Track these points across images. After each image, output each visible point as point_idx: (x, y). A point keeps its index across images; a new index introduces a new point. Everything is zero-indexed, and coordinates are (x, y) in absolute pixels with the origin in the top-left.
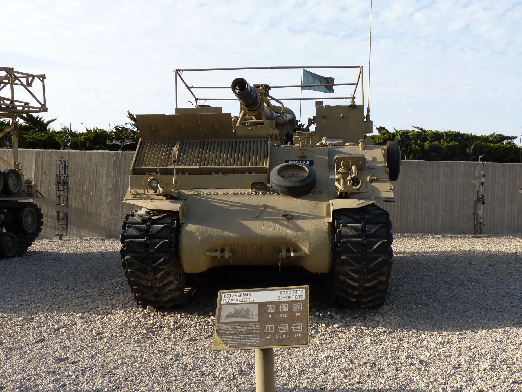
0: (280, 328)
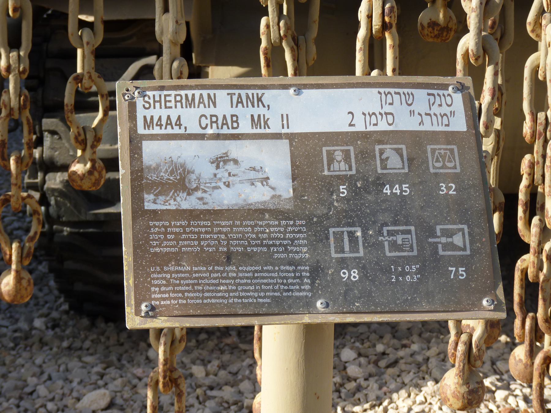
0: (385, 240)
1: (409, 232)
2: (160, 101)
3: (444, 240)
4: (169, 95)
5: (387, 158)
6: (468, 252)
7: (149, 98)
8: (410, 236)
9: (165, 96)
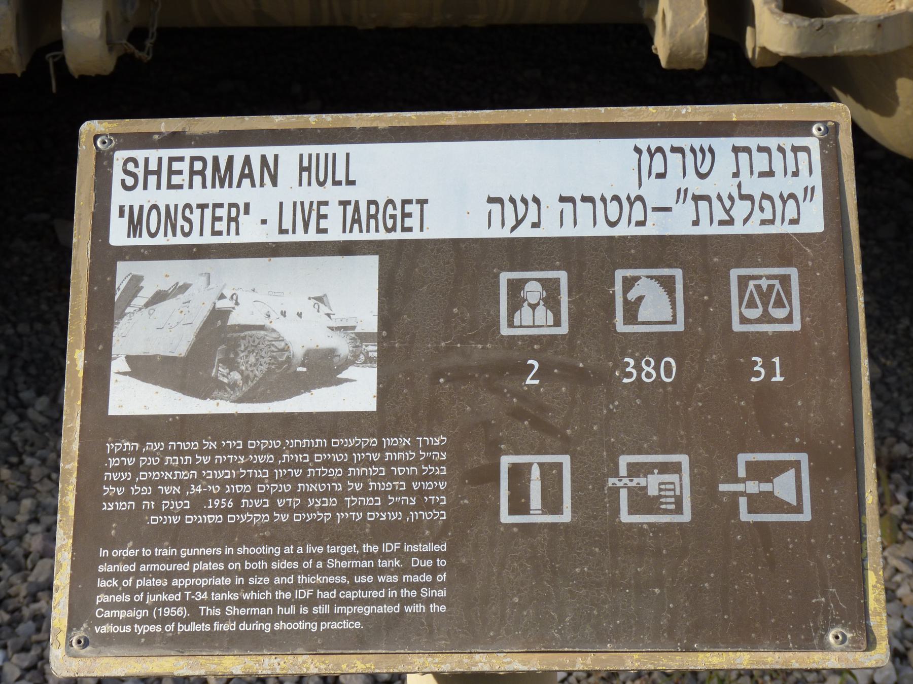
0: (622, 483)
1: (675, 468)
2: (158, 173)
3: (753, 487)
4: (181, 159)
5: (640, 299)
6: (806, 516)
7: (137, 166)
8: (677, 476)
9: (172, 160)
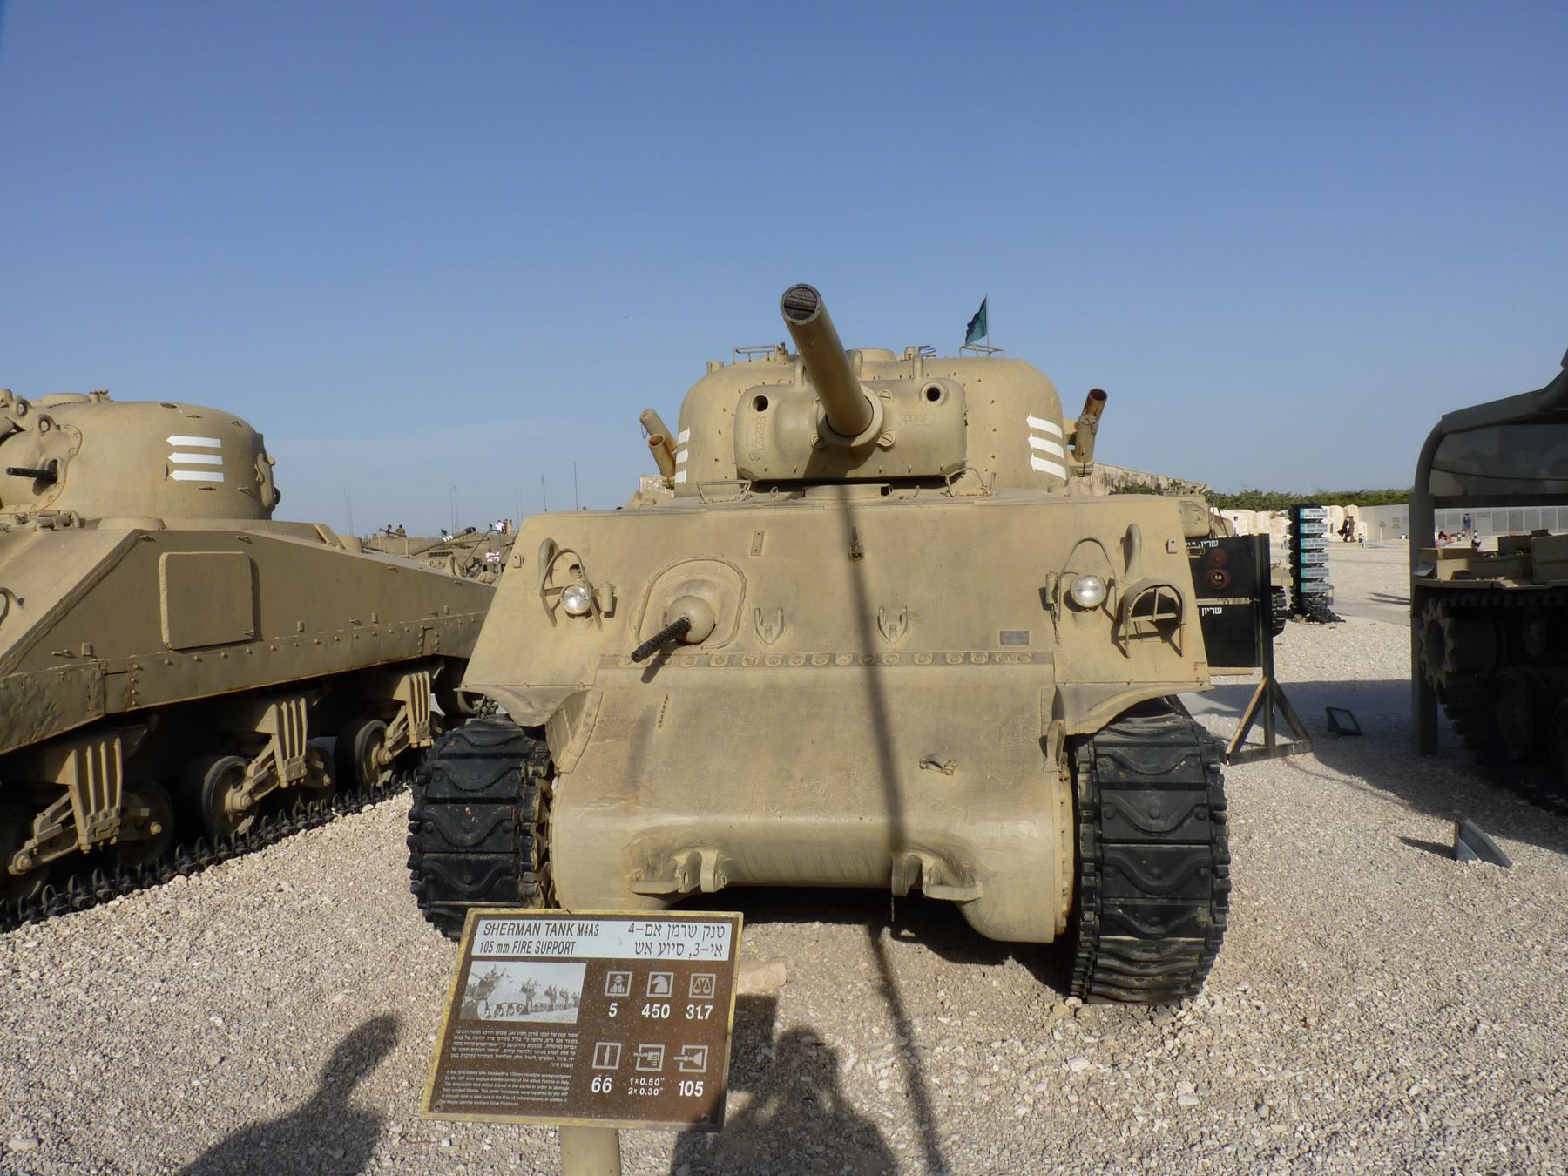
0: (639, 1055)
